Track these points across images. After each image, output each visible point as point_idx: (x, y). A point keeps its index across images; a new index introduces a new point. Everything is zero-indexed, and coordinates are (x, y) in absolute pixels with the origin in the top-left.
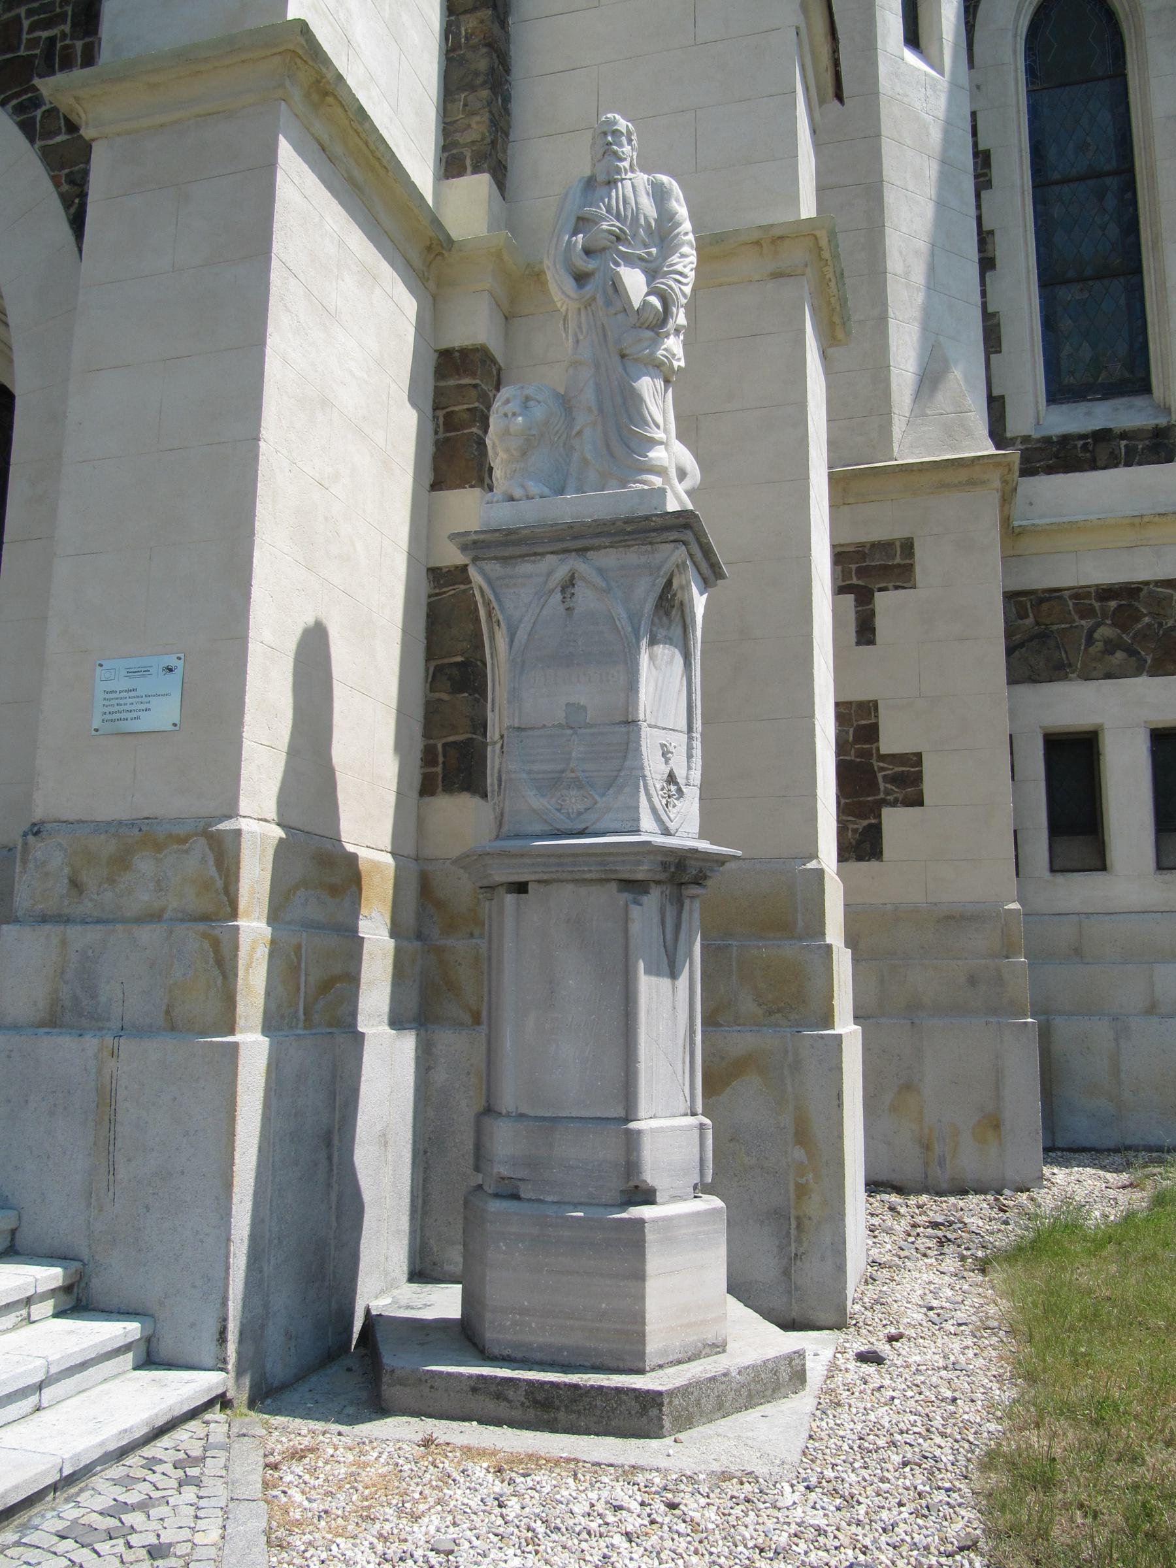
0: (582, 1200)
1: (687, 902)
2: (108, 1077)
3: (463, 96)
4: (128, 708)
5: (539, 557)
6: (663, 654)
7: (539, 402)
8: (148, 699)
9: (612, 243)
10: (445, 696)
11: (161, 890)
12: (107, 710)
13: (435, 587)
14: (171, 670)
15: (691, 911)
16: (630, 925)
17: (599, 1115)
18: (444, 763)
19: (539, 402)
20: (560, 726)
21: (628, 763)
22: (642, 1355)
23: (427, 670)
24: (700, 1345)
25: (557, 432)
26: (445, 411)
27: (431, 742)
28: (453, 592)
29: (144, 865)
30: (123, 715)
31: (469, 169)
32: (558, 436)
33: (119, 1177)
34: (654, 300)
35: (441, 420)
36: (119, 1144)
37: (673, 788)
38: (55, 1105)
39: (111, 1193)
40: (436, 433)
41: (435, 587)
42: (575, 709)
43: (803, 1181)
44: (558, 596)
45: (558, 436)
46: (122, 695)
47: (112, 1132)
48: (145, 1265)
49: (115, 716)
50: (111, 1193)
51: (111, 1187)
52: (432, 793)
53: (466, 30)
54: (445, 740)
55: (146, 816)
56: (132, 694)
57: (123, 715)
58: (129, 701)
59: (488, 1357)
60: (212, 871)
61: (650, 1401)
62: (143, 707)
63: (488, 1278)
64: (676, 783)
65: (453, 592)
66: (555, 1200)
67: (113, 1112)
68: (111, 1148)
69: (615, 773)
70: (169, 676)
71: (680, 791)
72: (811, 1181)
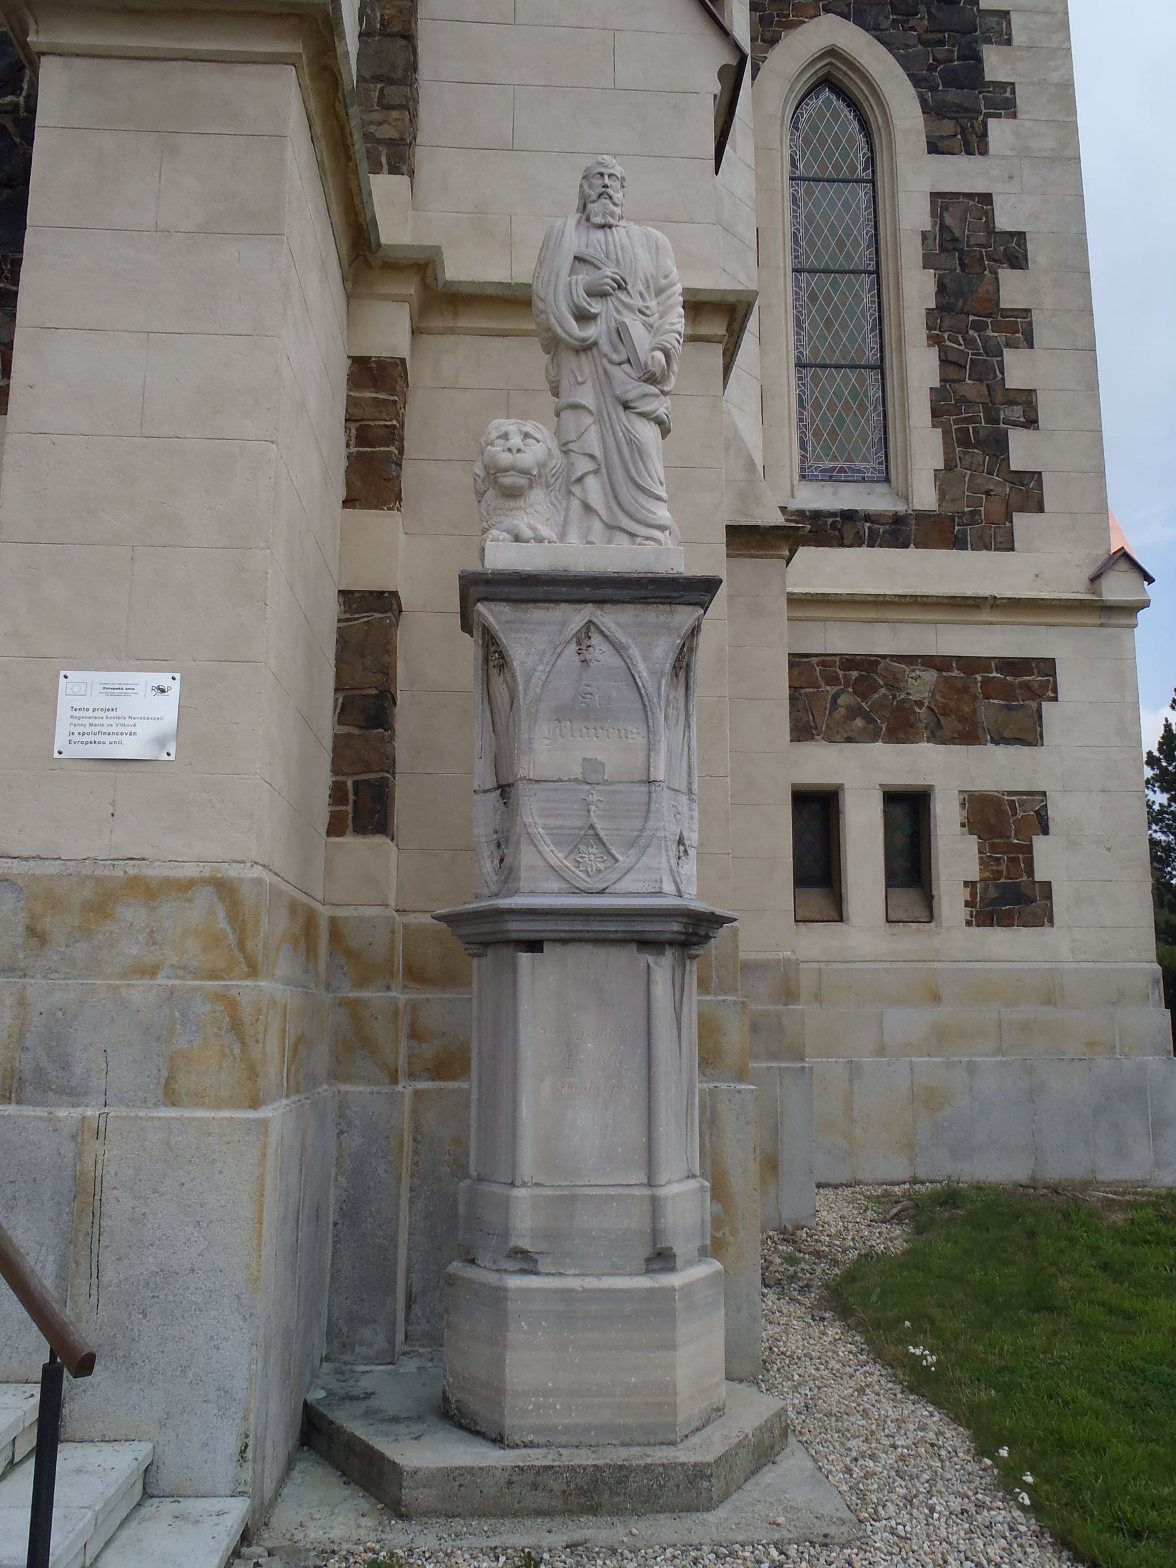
0: (606, 1271)
1: (688, 962)
2: (91, 1163)
3: (379, 86)
4: (104, 729)
5: (552, 605)
6: (673, 714)
7: (538, 441)
8: (132, 722)
9: (614, 290)
10: (356, 731)
11: (155, 943)
12: (76, 730)
13: (345, 612)
14: (163, 691)
15: (691, 973)
16: (652, 987)
17: (619, 1182)
18: (355, 801)
19: (538, 441)
20: (576, 780)
21: (650, 824)
22: (672, 1427)
23: (336, 700)
24: (710, 1410)
25: (553, 476)
26: (358, 424)
27: (339, 778)
28: (366, 619)
29: (132, 913)
30: (98, 738)
31: (385, 167)
32: (555, 478)
33: (105, 1279)
34: (660, 355)
35: (354, 432)
36: (105, 1240)
37: (682, 848)
38: (14, 1198)
39: (94, 1299)
40: (348, 446)
41: (345, 612)
42: (591, 765)
43: (719, 1235)
44: (573, 647)
45: (555, 478)
46: (97, 714)
47: (96, 1227)
48: (139, 1381)
49: (86, 738)
50: (94, 1299)
51: (94, 1292)
52: (341, 834)
53: (382, 16)
54: (356, 778)
55: (129, 856)
56: (110, 714)
57: (98, 738)
58: (105, 722)
59: (508, 1446)
60: (223, 924)
61: (698, 1473)
62: (128, 730)
63: (507, 1361)
64: (684, 844)
65: (366, 619)
66: (577, 1273)
67: (97, 1203)
68: (95, 1246)
69: (636, 833)
70: (162, 697)
71: (686, 852)
72: (728, 1234)
